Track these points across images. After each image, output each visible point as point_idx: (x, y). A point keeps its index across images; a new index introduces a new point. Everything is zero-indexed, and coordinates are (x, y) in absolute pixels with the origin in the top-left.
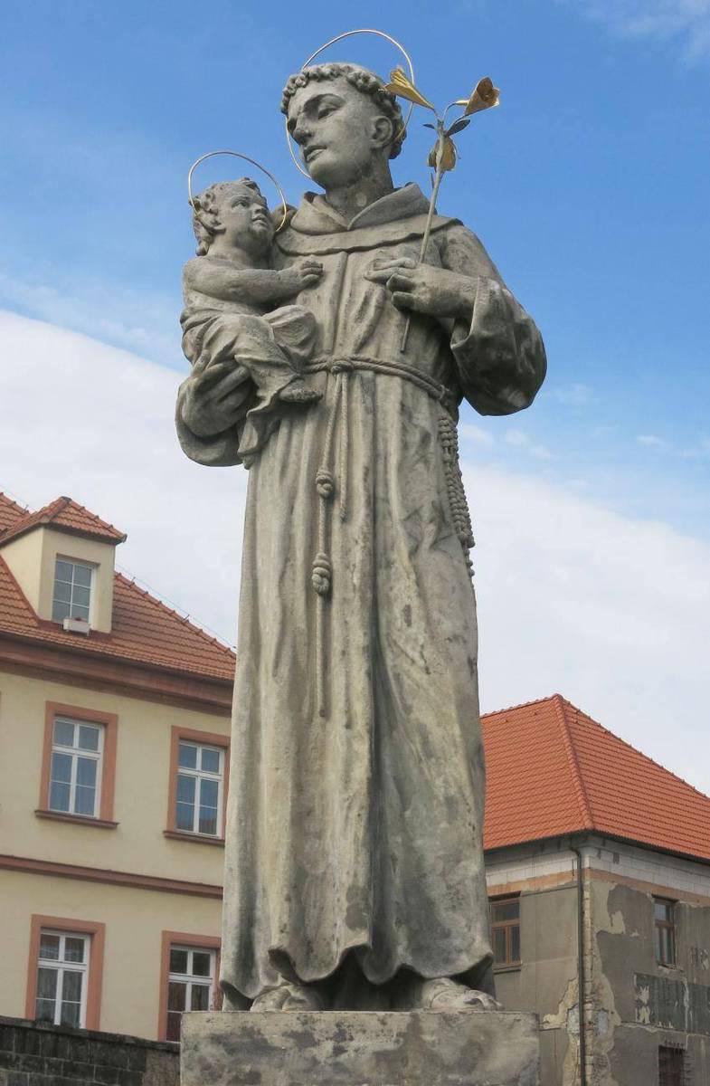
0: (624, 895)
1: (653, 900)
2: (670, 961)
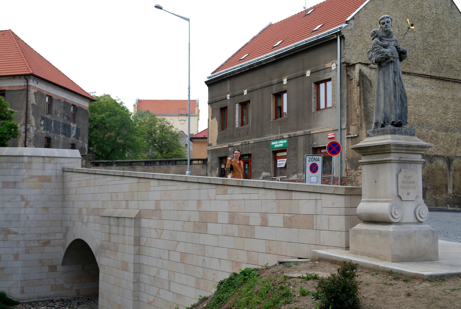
0: (39, 94)
1: (46, 96)
2: (48, 113)
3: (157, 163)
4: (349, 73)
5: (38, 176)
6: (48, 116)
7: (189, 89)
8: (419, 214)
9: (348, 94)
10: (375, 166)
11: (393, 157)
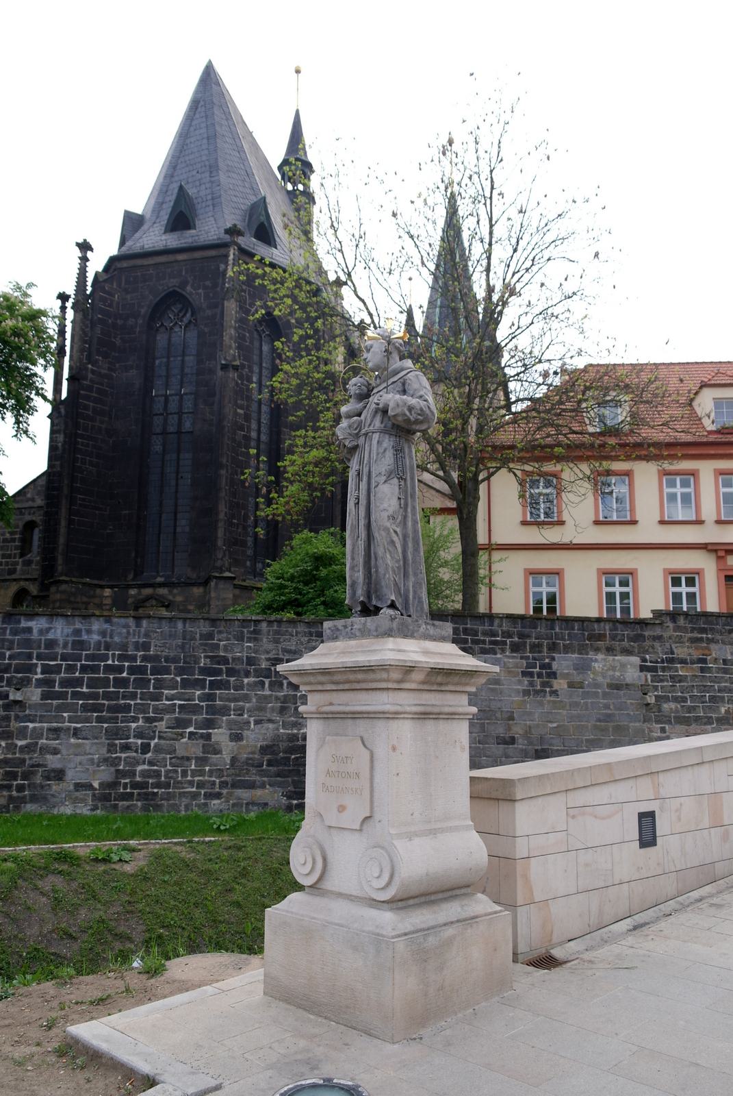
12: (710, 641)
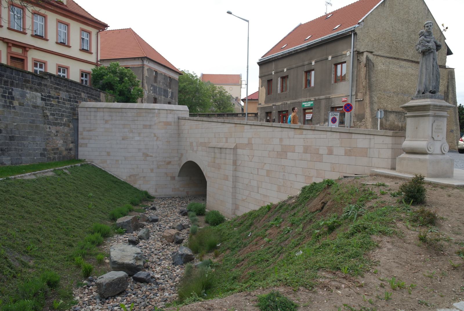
0: (150, 70)
3: (225, 115)
4: (359, 58)
5: (164, 122)
6: (155, 84)
7: (248, 67)
8: (444, 149)
9: (357, 72)
10: (417, 119)
11: (431, 113)
12: (60, 90)
